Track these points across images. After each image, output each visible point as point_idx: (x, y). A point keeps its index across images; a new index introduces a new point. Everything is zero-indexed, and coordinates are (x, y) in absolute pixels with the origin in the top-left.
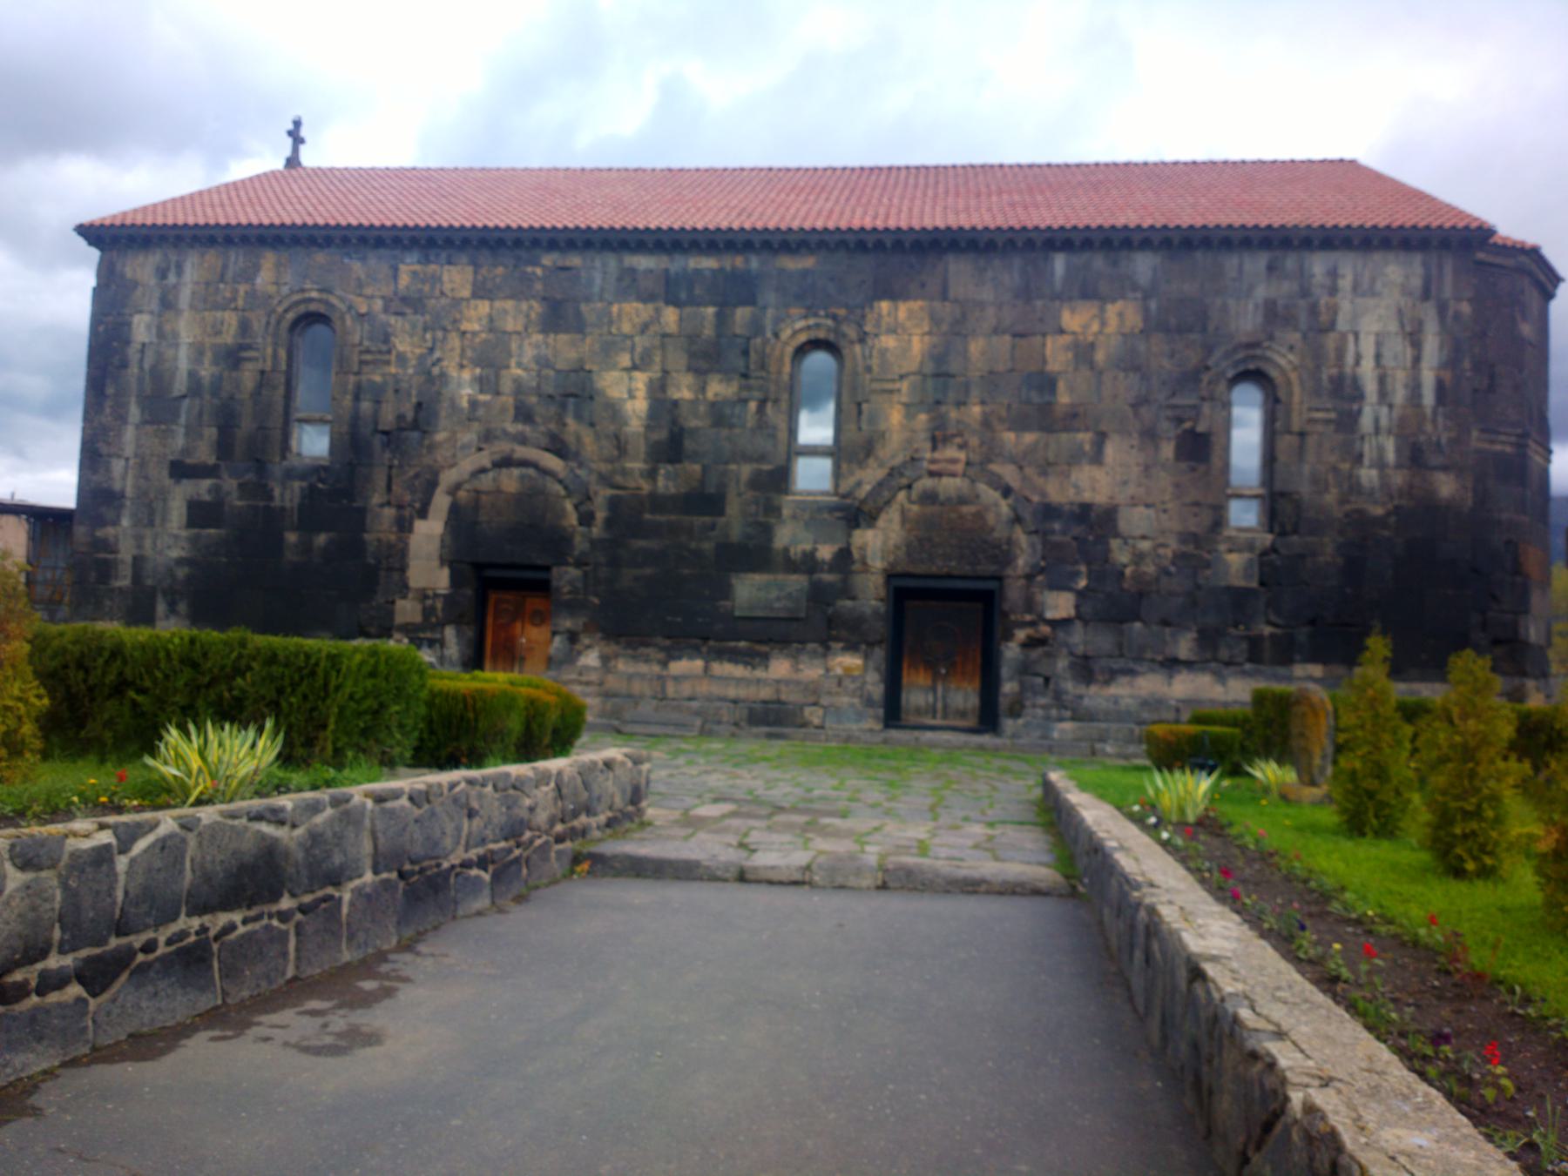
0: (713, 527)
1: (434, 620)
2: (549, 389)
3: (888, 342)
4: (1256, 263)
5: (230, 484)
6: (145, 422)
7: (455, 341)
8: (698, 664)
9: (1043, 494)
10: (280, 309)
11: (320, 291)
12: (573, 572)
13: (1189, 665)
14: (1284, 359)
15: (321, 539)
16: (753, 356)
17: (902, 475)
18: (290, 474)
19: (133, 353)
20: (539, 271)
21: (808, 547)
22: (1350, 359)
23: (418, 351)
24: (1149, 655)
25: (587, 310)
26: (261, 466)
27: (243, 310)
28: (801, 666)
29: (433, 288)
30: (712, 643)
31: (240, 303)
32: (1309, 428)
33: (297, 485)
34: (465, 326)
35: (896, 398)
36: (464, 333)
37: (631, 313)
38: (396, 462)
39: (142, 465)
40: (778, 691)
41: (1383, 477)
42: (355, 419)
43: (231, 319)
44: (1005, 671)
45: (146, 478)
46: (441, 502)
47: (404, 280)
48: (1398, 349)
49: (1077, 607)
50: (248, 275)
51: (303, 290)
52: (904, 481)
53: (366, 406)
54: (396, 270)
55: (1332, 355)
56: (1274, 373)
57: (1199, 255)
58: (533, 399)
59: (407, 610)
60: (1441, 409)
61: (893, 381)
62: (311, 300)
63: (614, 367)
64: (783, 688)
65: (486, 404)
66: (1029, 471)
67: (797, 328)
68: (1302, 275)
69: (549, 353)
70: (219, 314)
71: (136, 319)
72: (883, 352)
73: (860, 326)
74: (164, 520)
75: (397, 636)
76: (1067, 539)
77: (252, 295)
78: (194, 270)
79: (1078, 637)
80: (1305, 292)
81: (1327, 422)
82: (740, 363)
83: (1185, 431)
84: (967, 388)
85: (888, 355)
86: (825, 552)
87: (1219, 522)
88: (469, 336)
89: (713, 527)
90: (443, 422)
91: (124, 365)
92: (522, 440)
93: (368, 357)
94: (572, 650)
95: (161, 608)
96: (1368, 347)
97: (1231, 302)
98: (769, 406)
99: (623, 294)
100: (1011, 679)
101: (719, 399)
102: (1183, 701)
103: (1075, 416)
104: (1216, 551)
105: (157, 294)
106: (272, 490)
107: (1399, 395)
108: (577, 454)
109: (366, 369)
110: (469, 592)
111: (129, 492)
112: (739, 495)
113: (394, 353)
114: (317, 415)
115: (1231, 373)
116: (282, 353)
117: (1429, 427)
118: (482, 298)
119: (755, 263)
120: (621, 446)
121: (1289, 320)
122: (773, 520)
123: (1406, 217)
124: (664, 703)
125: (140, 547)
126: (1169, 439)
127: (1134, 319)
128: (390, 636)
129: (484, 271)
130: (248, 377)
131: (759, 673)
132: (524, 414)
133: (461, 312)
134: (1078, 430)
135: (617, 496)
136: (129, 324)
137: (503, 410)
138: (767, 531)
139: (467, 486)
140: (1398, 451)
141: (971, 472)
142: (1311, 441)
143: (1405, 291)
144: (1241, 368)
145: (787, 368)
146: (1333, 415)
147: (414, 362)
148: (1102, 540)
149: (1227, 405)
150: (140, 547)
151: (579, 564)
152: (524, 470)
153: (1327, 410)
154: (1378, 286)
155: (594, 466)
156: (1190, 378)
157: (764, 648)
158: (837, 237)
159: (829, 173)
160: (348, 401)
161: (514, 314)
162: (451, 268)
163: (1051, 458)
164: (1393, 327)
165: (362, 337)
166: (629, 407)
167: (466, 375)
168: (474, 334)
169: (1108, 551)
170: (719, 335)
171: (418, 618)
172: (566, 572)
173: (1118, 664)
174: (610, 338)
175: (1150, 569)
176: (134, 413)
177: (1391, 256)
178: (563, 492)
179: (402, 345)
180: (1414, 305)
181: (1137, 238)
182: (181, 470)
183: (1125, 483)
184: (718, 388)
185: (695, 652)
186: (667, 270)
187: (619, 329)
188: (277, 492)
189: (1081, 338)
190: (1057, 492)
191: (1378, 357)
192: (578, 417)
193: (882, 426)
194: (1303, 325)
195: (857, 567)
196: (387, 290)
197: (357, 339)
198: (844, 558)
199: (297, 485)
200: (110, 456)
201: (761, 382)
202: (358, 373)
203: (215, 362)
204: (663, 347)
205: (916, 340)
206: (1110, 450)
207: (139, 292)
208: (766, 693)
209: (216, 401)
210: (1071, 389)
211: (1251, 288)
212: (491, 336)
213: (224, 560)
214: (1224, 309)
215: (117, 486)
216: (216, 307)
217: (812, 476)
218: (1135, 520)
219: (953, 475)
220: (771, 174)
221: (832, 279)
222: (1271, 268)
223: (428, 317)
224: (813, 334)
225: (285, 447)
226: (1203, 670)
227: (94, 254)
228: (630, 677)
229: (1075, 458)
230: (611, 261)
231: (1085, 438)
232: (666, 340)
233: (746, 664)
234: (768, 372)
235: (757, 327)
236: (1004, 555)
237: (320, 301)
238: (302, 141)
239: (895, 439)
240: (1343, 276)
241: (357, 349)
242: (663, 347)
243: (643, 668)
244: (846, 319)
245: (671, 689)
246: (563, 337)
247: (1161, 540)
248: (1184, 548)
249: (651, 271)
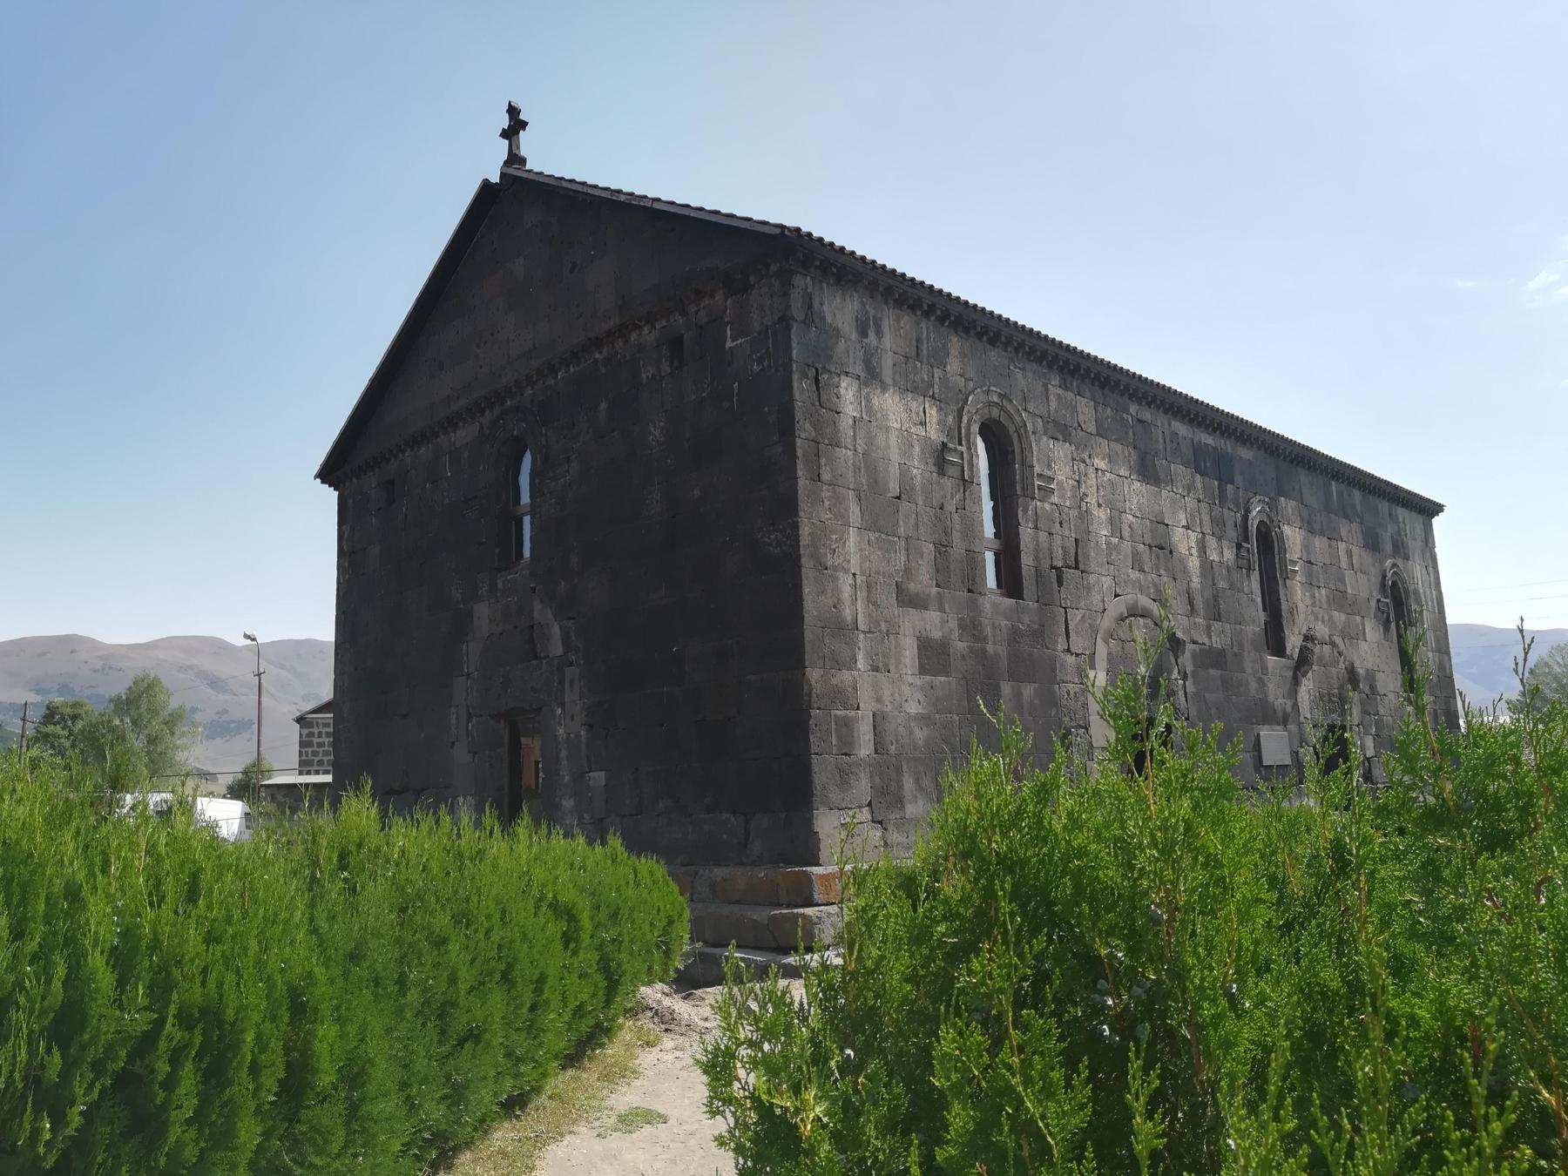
7: (1092, 480)
36: (1097, 469)
47: (1053, 404)
50: (939, 358)
53: (1043, 535)
54: (1047, 390)
74: (898, 661)
90: (1093, 566)
95: (908, 784)
118: (1102, 437)
125: (879, 700)
147: (1069, 494)
150: (879, 700)
162: (1082, 399)
215: (847, 614)
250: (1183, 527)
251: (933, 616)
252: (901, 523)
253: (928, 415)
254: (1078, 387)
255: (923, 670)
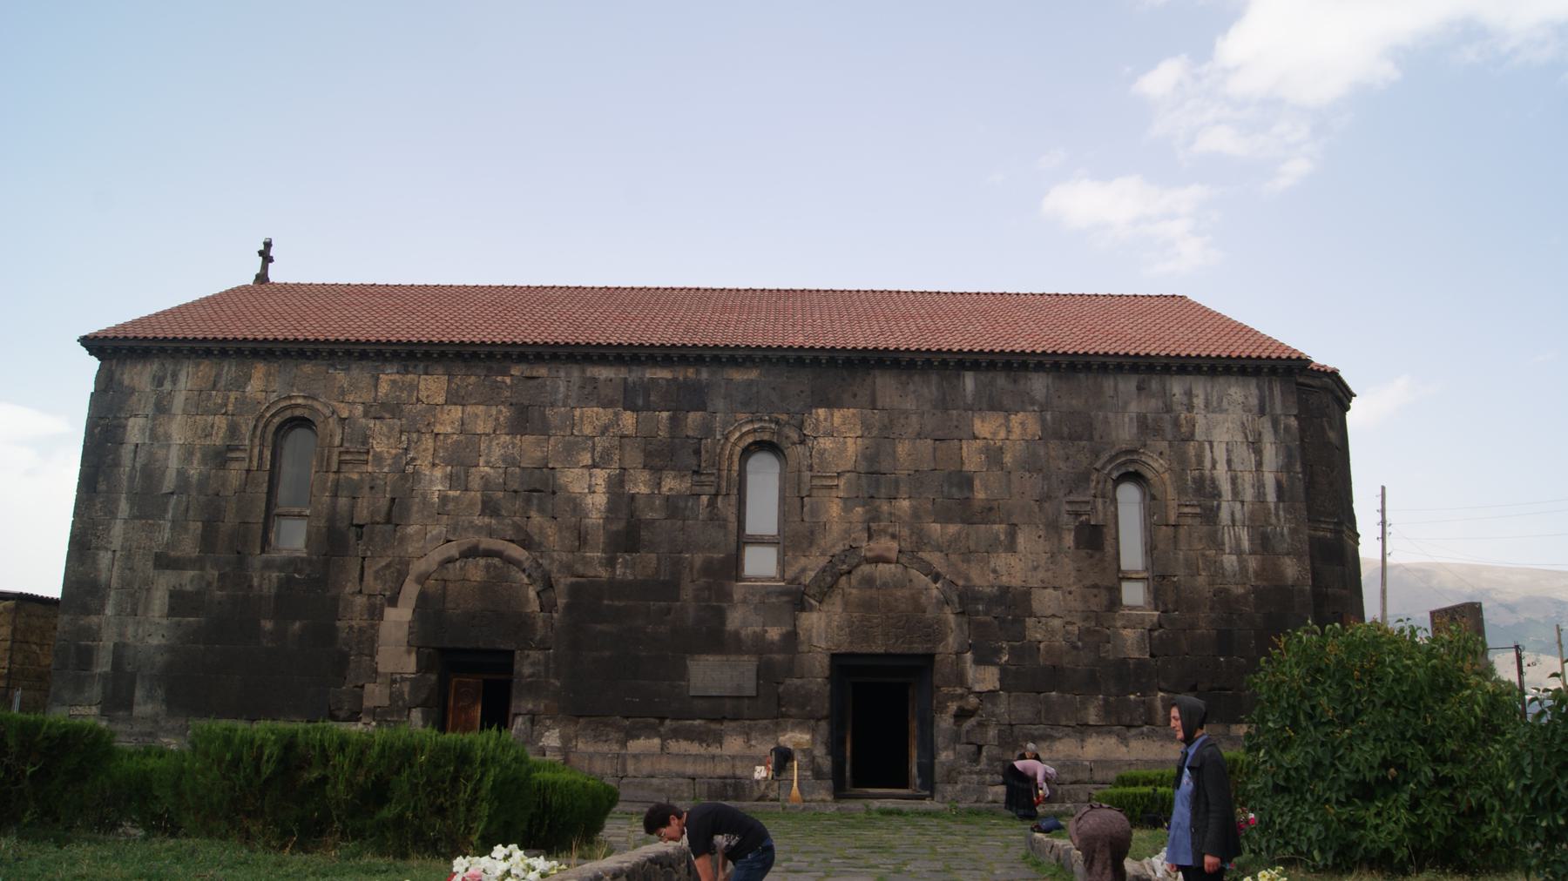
0: (669, 611)
1: (400, 703)
2: (516, 487)
3: (826, 443)
4: (1128, 384)
5: (213, 574)
6: (134, 517)
7: (428, 442)
8: (657, 741)
9: (967, 579)
10: (268, 415)
11: (304, 397)
12: (535, 655)
13: (1099, 729)
14: (1156, 464)
15: (297, 625)
16: (704, 456)
17: (844, 562)
18: (268, 565)
19: (126, 453)
20: (508, 380)
21: (758, 629)
22: (1208, 464)
23: (394, 451)
24: (1064, 723)
25: (554, 415)
26: (241, 559)
27: (233, 415)
28: (753, 742)
29: (410, 396)
30: (668, 722)
31: (230, 408)
32: (1183, 520)
33: (274, 575)
34: (438, 429)
35: (834, 493)
36: (437, 434)
37: (592, 417)
38: (369, 554)
39: (129, 556)
40: (733, 766)
41: (1240, 561)
42: (332, 517)
43: (221, 422)
44: (940, 741)
45: (130, 569)
46: (411, 590)
47: (384, 388)
48: (1244, 456)
49: (1001, 680)
50: (240, 384)
51: (290, 398)
52: (845, 567)
53: (343, 501)
54: (378, 379)
55: (1193, 459)
56: (1149, 474)
57: (1082, 376)
58: (501, 494)
59: (375, 695)
60: (1281, 505)
61: (831, 477)
62: (298, 406)
63: (576, 465)
64: (738, 763)
65: (455, 499)
66: (953, 557)
67: (744, 430)
68: (1164, 394)
69: (516, 452)
70: (211, 417)
71: (131, 421)
72: (822, 453)
73: (800, 427)
74: (147, 609)
75: (364, 720)
76: (988, 619)
77: (242, 402)
78: (188, 379)
79: (1002, 707)
80: (1168, 409)
81: (1195, 515)
82: (693, 461)
83: (1082, 522)
84: (897, 483)
85: (826, 455)
86: (774, 633)
87: (1115, 602)
88: (441, 437)
89: (669, 611)
90: (415, 516)
91: (116, 464)
92: (491, 533)
93: (348, 457)
94: (532, 731)
96: (1221, 454)
97: (1111, 415)
98: (720, 498)
99: (584, 401)
100: (946, 748)
101: (674, 493)
102: (1095, 761)
103: (991, 509)
104: (1115, 627)
105: (153, 400)
106: (251, 580)
107: (1249, 494)
108: (540, 544)
109: (344, 468)
110: (433, 677)
111: (114, 582)
112: (693, 581)
113: (371, 453)
114: (296, 510)
115: (1115, 475)
116: (267, 454)
117: (1273, 520)
118: (455, 404)
119: (705, 375)
120: (581, 538)
121: (1158, 431)
122: (725, 605)
123: (1240, 349)
124: (625, 781)
125: (121, 635)
126: (1068, 530)
127: (1034, 428)
128: (358, 720)
129: (457, 380)
130: (235, 474)
131: (714, 750)
132: (489, 508)
133: (434, 416)
134: (994, 523)
135: (577, 582)
136: (125, 427)
137: (472, 504)
138: (720, 615)
139: (435, 576)
140: (1251, 540)
141: (903, 559)
142: (1183, 531)
143: (1246, 409)
144: (1123, 470)
145: (736, 467)
146: (1198, 510)
147: (389, 462)
148: (1019, 621)
149: (1114, 501)
150: (121, 635)
151: (542, 646)
152: (489, 560)
153: (1192, 506)
154: (1225, 404)
155: (555, 555)
156: (1082, 479)
157: (714, 726)
158: (780, 354)
159: (750, 293)
160: (326, 498)
161: (483, 418)
163: (972, 548)
164: (1239, 438)
165: (342, 439)
166: (589, 500)
167: (438, 473)
168: (446, 435)
169: (1024, 628)
170: (672, 437)
171: (387, 703)
172: (528, 656)
173: (1037, 730)
174: (572, 438)
175: (1059, 642)
176: (124, 508)
177: (1233, 380)
178: (526, 580)
179: (379, 446)
180: (1253, 420)
181: (1032, 361)
182: (164, 562)
183: (1035, 568)
184: (670, 484)
185: (651, 731)
186: (626, 379)
187: (580, 431)
188: (256, 582)
189: (992, 442)
190: (981, 579)
191: (1229, 462)
192: (541, 511)
193: (823, 519)
194: (1170, 437)
195: (804, 648)
196: (368, 397)
197: (337, 441)
198: (791, 638)
199: (274, 575)
200: (97, 548)
201: (712, 478)
202: (338, 472)
203: (204, 461)
204: (621, 447)
205: (850, 441)
206: (1021, 539)
207: (135, 398)
208: (722, 769)
209: (202, 498)
210: (986, 488)
211: (1126, 404)
212: (462, 437)
213: (202, 647)
214: (1106, 421)
215: (103, 577)
216: (207, 412)
217: (760, 563)
218: (1046, 601)
219: (887, 561)
220: (700, 293)
221: (774, 388)
222: (1140, 388)
223: (404, 421)
224: (759, 437)
225: (265, 543)
226: (1110, 733)
227: (94, 363)
228: (591, 757)
229: (993, 546)
230: (576, 373)
231: (999, 528)
232: (623, 440)
233: (701, 741)
234: (719, 470)
235: (708, 430)
236: (934, 633)
237: (304, 406)
238: (261, 253)
239: (836, 529)
240: (1197, 396)
241: (336, 451)
242: (621, 447)
243: (604, 748)
244: (787, 423)
245: (631, 768)
246: (529, 438)
247: (1069, 619)
248: (1087, 625)
249: (611, 380)
250: (583, 467)
251: (190, 573)
252: (171, 512)
253: (216, 428)
254: (426, 367)
255: (173, 611)
